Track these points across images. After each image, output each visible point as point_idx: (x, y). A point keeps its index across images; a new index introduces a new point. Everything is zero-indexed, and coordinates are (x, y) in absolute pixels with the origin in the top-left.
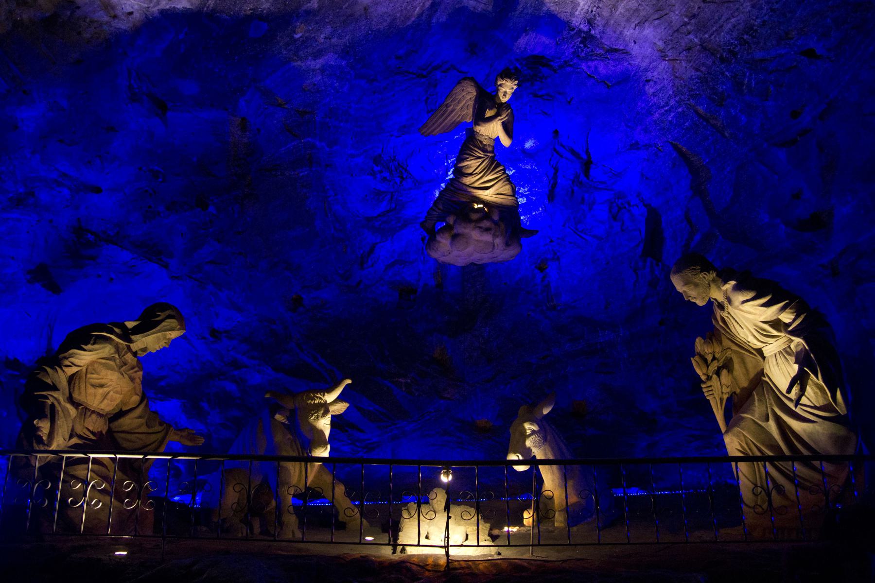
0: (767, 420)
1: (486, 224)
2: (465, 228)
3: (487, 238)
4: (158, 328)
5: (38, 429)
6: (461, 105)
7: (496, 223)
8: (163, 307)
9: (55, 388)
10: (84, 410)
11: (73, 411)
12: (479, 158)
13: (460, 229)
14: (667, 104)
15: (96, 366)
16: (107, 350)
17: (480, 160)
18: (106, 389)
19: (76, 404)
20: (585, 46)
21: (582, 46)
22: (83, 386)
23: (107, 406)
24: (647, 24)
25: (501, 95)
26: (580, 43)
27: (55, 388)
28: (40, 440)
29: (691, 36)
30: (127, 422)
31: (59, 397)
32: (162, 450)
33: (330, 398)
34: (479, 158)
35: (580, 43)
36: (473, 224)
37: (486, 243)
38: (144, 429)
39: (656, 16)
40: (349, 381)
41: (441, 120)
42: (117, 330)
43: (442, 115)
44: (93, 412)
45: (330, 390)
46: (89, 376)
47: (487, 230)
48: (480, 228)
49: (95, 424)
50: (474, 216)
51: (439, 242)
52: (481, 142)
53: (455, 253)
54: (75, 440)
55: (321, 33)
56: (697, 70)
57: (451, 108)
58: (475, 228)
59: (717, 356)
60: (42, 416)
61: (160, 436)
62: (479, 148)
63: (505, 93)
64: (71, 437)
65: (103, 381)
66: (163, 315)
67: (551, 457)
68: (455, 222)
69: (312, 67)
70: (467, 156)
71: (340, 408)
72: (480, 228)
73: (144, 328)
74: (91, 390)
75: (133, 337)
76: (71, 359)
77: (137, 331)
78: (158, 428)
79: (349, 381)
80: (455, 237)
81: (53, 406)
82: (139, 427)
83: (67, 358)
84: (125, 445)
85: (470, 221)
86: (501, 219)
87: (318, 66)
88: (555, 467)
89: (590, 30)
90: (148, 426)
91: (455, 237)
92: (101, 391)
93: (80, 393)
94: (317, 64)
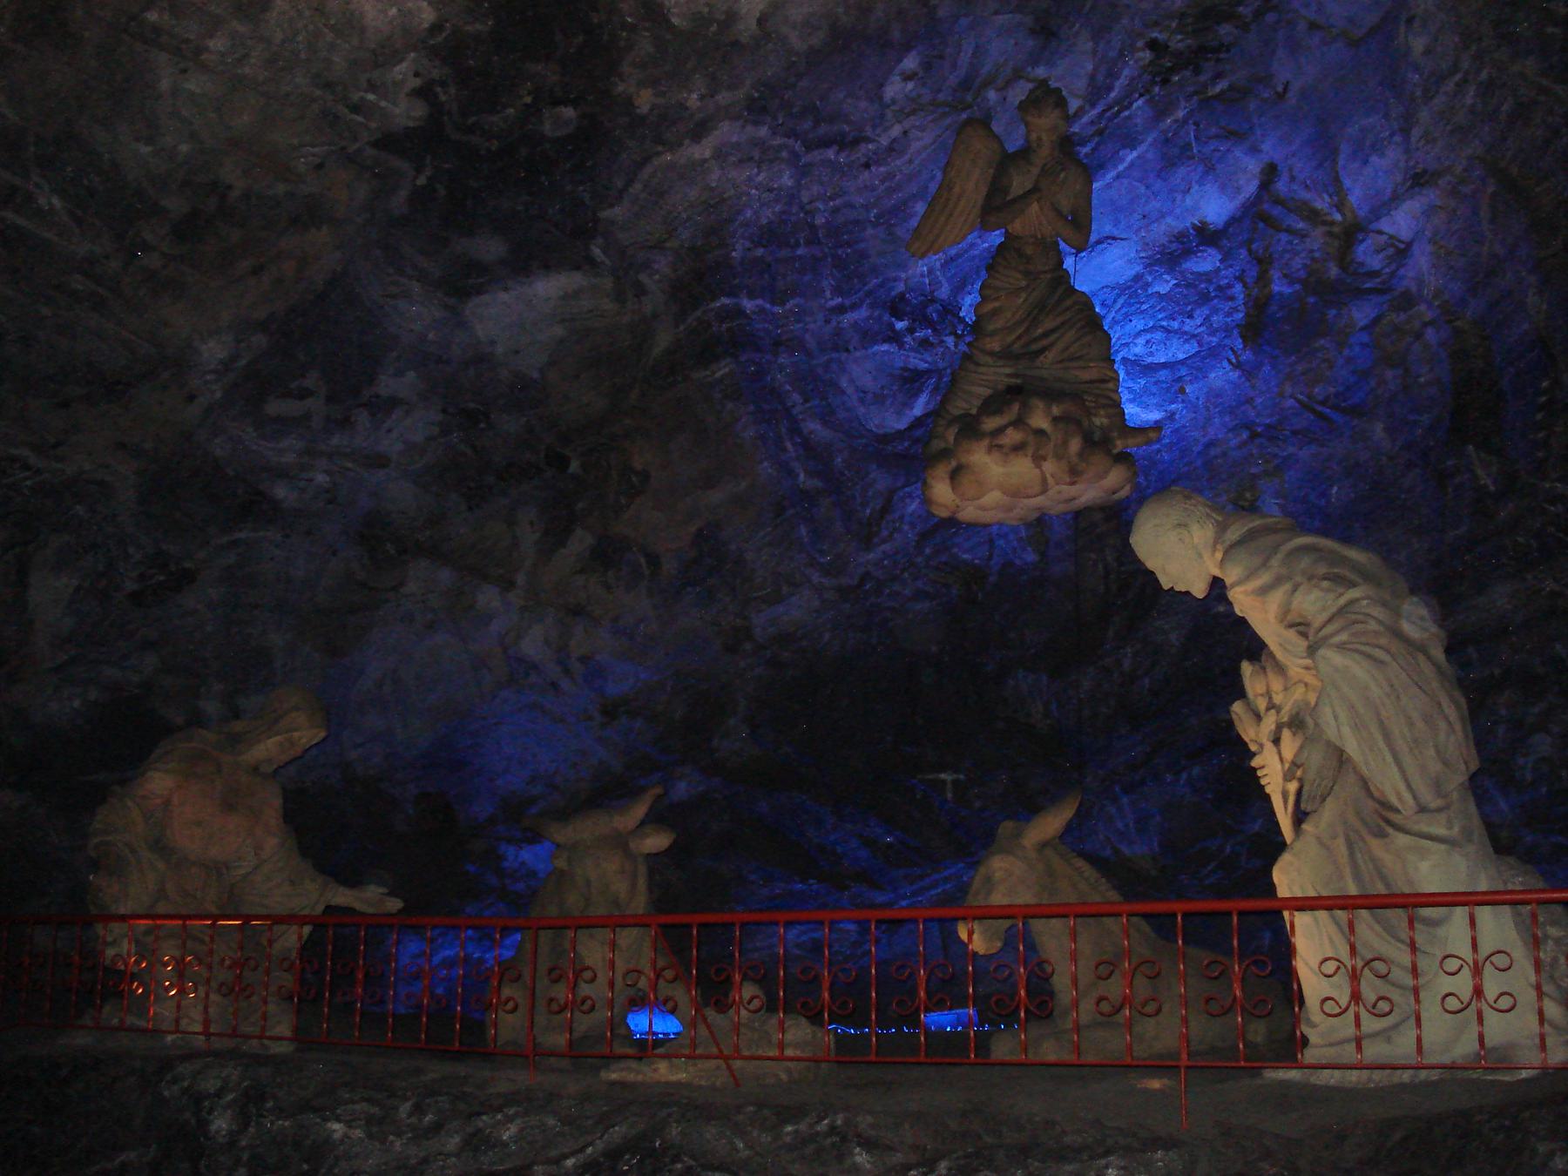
0: (1334, 837)
14: (1455, 69)
36: (986, 442)
47: (1018, 448)
57: (957, 189)
58: (990, 450)
59: (1277, 699)
69: (697, 156)
87: (707, 154)
94: (702, 150)
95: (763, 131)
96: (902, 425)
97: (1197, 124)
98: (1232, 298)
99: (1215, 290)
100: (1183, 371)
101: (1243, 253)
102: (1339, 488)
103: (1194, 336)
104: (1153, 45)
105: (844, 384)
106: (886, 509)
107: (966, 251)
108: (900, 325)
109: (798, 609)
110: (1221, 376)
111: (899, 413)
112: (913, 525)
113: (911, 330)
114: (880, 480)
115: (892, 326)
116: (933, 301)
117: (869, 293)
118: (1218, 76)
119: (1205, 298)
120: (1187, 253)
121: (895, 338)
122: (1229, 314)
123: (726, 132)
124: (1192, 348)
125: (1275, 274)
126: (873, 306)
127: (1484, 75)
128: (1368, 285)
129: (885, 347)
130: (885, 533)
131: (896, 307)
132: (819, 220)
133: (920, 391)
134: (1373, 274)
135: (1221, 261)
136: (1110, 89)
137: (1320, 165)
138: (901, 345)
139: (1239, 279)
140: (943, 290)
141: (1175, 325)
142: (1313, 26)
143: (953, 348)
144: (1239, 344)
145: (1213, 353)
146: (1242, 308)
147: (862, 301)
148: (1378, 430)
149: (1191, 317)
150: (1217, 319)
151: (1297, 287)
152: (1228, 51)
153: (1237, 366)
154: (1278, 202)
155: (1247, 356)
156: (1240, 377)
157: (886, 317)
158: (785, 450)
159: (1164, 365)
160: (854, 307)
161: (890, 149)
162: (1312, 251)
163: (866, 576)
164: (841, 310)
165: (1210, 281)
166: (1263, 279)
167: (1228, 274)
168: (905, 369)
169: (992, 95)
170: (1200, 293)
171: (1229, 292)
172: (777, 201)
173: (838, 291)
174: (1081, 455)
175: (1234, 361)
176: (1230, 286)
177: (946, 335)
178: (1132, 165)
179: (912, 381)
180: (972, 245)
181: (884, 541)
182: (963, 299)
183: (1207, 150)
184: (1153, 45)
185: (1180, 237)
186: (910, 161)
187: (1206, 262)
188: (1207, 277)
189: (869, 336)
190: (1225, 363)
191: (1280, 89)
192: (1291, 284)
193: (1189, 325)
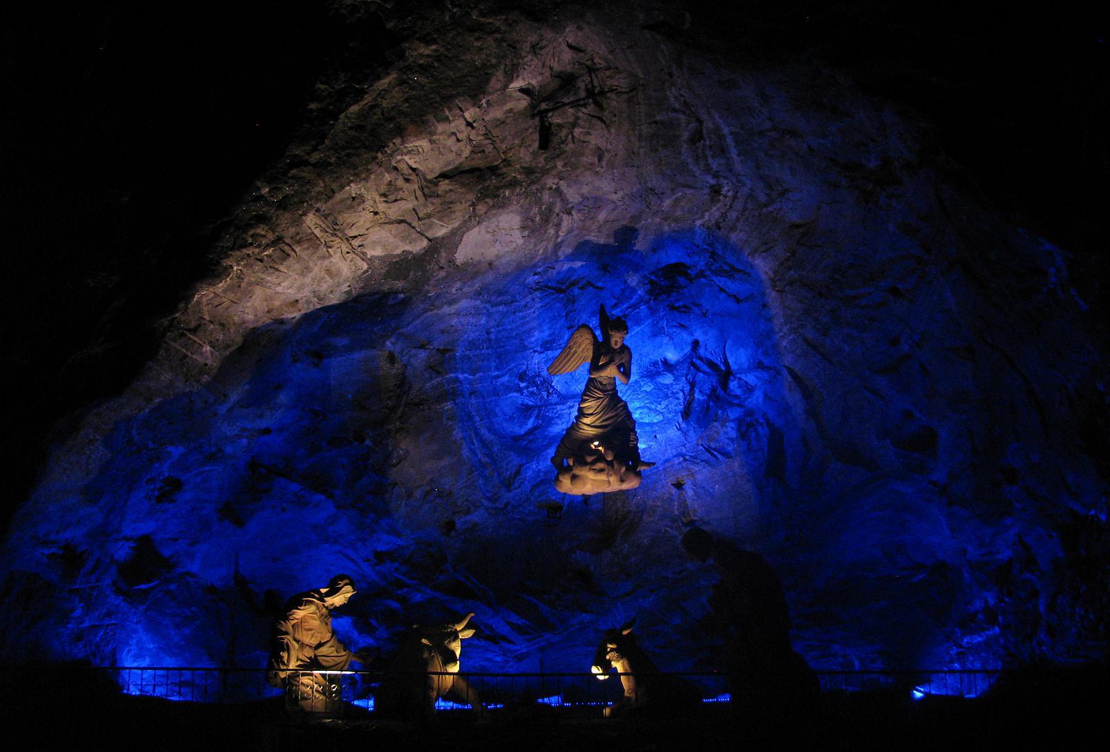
1: (600, 465)
2: (581, 470)
3: (602, 477)
4: (340, 592)
5: (282, 657)
6: (581, 348)
7: (610, 464)
8: (342, 578)
9: (287, 633)
10: (303, 645)
11: (296, 646)
12: (599, 398)
13: (577, 471)
15: (307, 618)
16: (312, 608)
17: (601, 400)
18: (313, 632)
19: (297, 641)
20: (715, 260)
22: (300, 629)
23: (314, 642)
24: (756, 255)
25: (613, 344)
26: (710, 257)
27: (287, 633)
28: (283, 663)
29: (792, 272)
30: (324, 650)
31: (288, 639)
32: (346, 667)
33: (459, 627)
34: (599, 398)
35: (710, 257)
36: (588, 467)
37: (604, 481)
38: (335, 654)
39: (763, 249)
40: (473, 615)
41: (566, 360)
42: (316, 595)
43: (567, 356)
44: (307, 645)
45: (459, 621)
46: (303, 624)
47: (601, 471)
49: (309, 653)
50: (589, 459)
51: (560, 481)
52: (601, 383)
54: (299, 663)
55: (453, 288)
56: (801, 302)
58: (590, 470)
60: (283, 651)
61: (345, 658)
62: (599, 389)
63: (616, 342)
64: (297, 661)
65: (311, 627)
66: (342, 583)
67: (629, 671)
69: (448, 312)
70: (588, 398)
71: (469, 634)
73: (333, 592)
74: (305, 633)
75: (326, 599)
76: (294, 616)
77: (329, 594)
78: (344, 653)
79: (473, 615)
80: (574, 478)
81: (287, 644)
82: (331, 653)
83: (290, 615)
84: (325, 664)
86: (615, 458)
88: (631, 677)
90: (337, 652)
91: (574, 478)
92: (310, 633)
93: (299, 635)
94: (453, 309)
95: (478, 302)
96: (522, 432)
97: (667, 319)
98: (678, 399)
99: (671, 394)
100: (656, 428)
101: (684, 378)
103: (661, 413)
104: (651, 282)
105: (497, 410)
106: (518, 473)
108: (522, 385)
109: (477, 517)
110: (673, 433)
111: (521, 427)
112: (529, 482)
113: (527, 387)
114: (514, 460)
115: (519, 385)
116: (539, 376)
117: (509, 370)
118: (678, 300)
119: (667, 397)
120: (658, 374)
121: (520, 391)
122: (676, 406)
123: (464, 303)
124: (660, 418)
125: (697, 391)
126: (511, 375)
127: (791, 337)
129: (515, 394)
130: (516, 485)
131: (522, 377)
132: (492, 336)
133: (530, 416)
134: (737, 397)
135: (674, 380)
136: (631, 299)
138: (522, 394)
139: (683, 391)
141: (653, 407)
143: (546, 398)
144: (681, 420)
145: (668, 422)
146: (682, 404)
147: (506, 373)
149: (660, 404)
150: (672, 407)
151: (705, 397)
153: (680, 429)
154: (700, 358)
157: (517, 381)
158: (473, 444)
159: (648, 424)
160: (503, 375)
161: (526, 306)
163: (508, 504)
164: (498, 377)
165: (668, 388)
167: (677, 388)
168: (522, 404)
170: (663, 393)
171: (677, 396)
172: (478, 330)
173: (497, 369)
174: (624, 473)
176: (677, 393)
178: (638, 332)
179: (526, 410)
181: (516, 489)
183: (671, 331)
184: (651, 282)
185: (655, 364)
187: (668, 379)
188: (668, 387)
189: (508, 389)
190: (675, 427)
191: (704, 311)
192: (703, 396)
193: (659, 408)
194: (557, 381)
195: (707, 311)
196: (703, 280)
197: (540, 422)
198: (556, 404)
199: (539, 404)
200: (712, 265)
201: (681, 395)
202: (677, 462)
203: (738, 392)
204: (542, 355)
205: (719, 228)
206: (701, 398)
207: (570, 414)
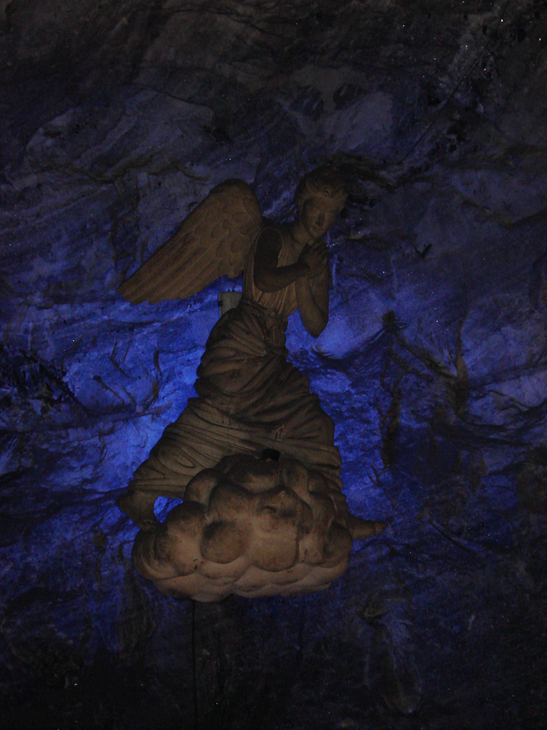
2: (238, 509)
20: (460, 139)
21: (453, 137)
48: (273, 510)
53: (212, 567)
58: (260, 510)
68: (214, 494)
72: (273, 510)
85: (250, 495)
89: (475, 104)
97: (340, 259)
98: (367, 422)
99: (348, 410)
101: (377, 382)
102: (477, 617)
107: (83, 319)
116: (33, 359)
118: (359, 225)
128: (492, 436)
135: (352, 386)
137: (447, 324)
139: (375, 404)
140: (48, 350)
142: (467, 204)
143: (39, 412)
144: (380, 464)
146: (378, 432)
148: (521, 567)
151: (425, 424)
152: (372, 204)
153: (378, 484)
155: (386, 476)
156: (380, 495)
162: (436, 396)
165: (342, 402)
166: (393, 412)
169: (143, 177)
175: (374, 478)
177: (33, 398)
180: (91, 315)
182: (70, 365)
186: (38, 215)
188: (336, 397)
190: (368, 480)
191: (421, 249)
194: (76, 373)
195: (428, 248)
196: (420, 186)
197: (28, 463)
198: (67, 426)
199: (20, 427)
200: (453, 148)
201: (373, 414)
202: (373, 556)
203: (498, 419)
204: (47, 314)
205: (521, 35)
206: (415, 425)
207: (105, 446)
